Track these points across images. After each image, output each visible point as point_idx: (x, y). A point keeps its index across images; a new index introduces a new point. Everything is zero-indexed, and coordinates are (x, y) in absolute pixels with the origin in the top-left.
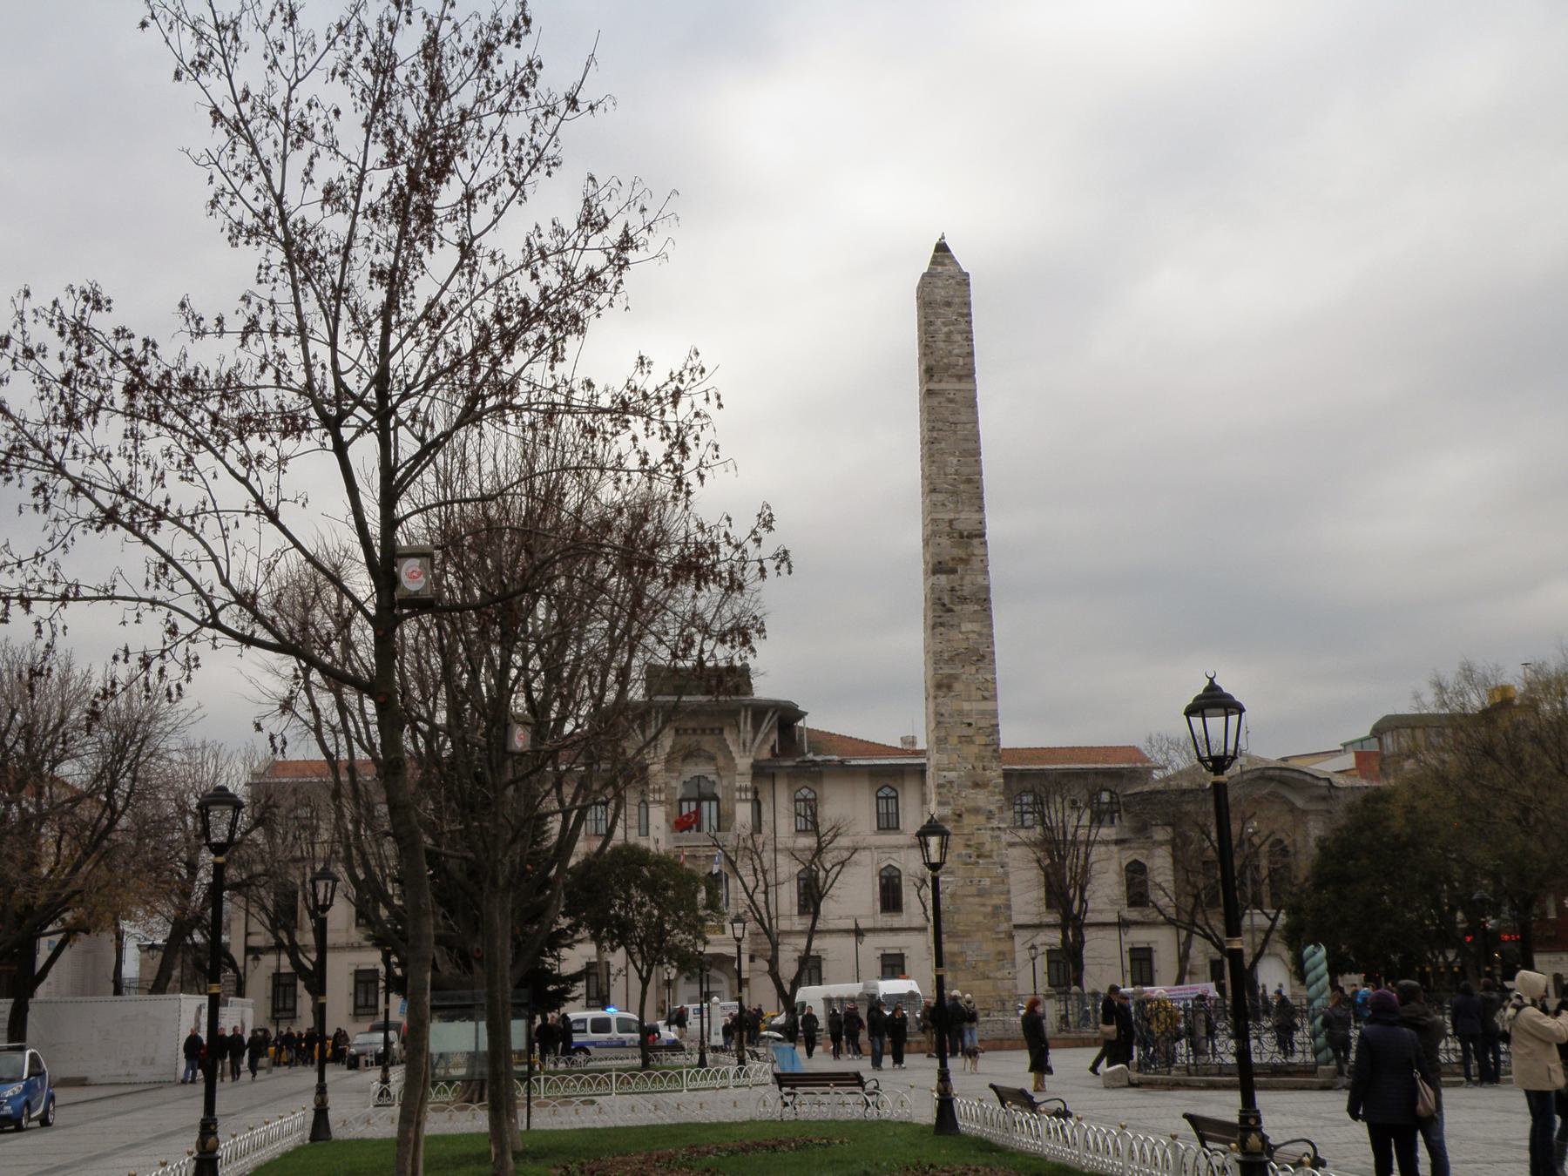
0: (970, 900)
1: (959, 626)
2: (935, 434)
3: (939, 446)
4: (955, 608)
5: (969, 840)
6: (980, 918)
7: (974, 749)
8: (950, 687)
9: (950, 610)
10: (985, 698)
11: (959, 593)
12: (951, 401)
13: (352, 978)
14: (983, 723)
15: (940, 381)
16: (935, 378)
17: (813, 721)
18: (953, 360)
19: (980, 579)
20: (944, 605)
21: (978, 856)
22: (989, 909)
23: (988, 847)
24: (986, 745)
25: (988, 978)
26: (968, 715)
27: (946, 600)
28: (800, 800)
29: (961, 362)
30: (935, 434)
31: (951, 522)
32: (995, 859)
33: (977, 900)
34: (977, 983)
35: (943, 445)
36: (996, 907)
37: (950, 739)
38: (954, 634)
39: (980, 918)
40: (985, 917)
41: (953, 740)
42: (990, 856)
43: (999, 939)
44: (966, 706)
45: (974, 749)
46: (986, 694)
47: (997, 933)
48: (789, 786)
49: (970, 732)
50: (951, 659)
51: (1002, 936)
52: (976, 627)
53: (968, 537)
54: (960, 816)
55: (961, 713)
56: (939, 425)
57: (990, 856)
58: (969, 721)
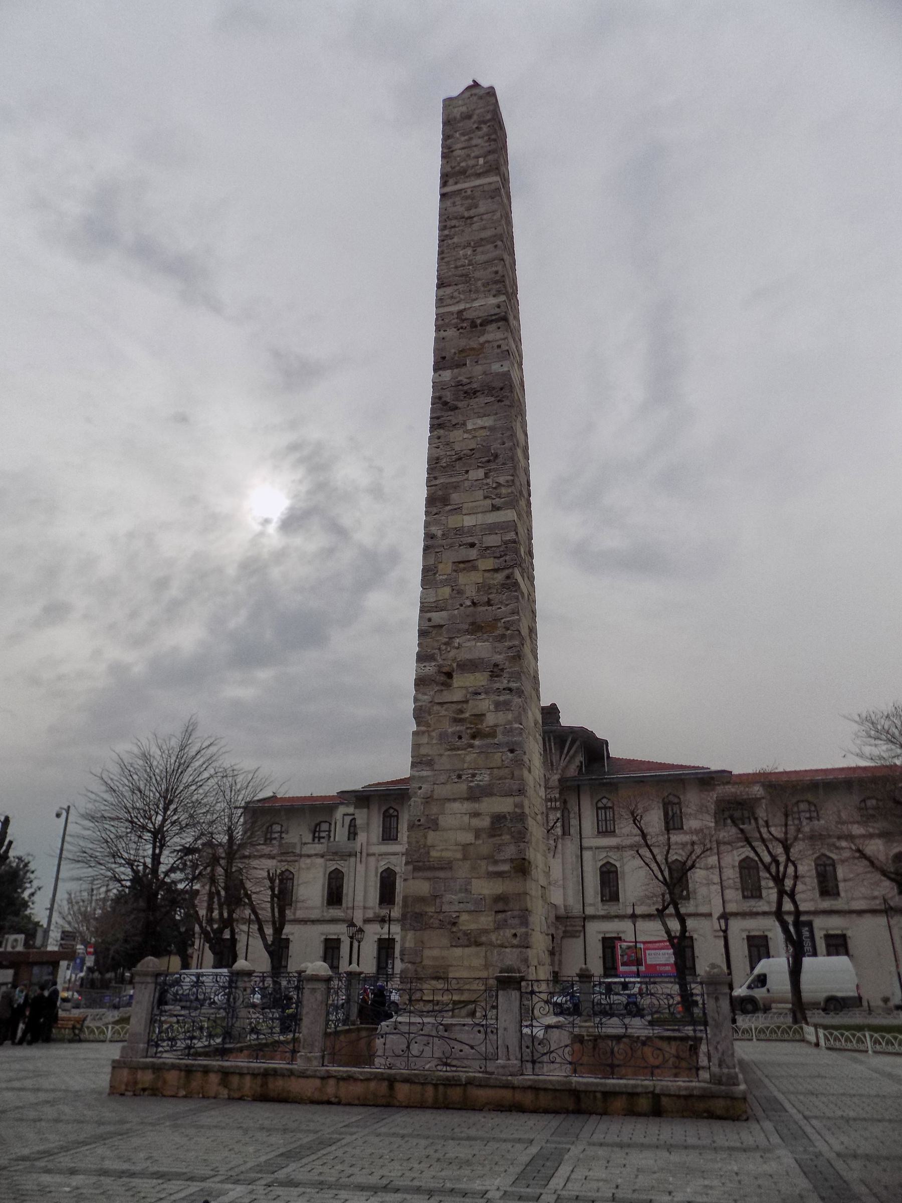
0: (456, 806)
1: (464, 424)
2: (446, 232)
3: (450, 242)
4: (460, 404)
5: (461, 711)
6: (469, 838)
7: (476, 577)
8: (445, 501)
9: (456, 408)
10: (495, 508)
11: (465, 388)
12: (467, 198)
13: (375, 946)
14: (493, 540)
15: (456, 183)
16: (451, 181)
17: (616, 751)
18: (471, 162)
19: (496, 367)
20: (446, 403)
21: (474, 737)
22: (486, 822)
23: (491, 719)
24: (496, 570)
25: (478, 944)
26: (471, 531)
27: (448, 396)
28: (601, 808)
29: (481, 161)
30: (446, 232)
31: (460, 312)
32: (500, 738)
33: (467, 806)
34: (458, 951)
35: (455, 240)
36: (498, 819)
37: (441, 566)
38: (456, 435)
39: (469, 838)
40: (477, 837)
41: (446, 568)
42: (493, 735)
43: (500, 875)
44: (468, 521)
45: (476, 577)
46: (498, 501)
47: (496, 862)
48: (592, 797)
49: (473, 554)
50: (451, 466)
51: (505, 867)
52: (488, 422)
53: (481, 325)
54: (449, 675)
55: (459, 531)
56: (454, 222)
57: (493, 735)
58: (470, 540)
